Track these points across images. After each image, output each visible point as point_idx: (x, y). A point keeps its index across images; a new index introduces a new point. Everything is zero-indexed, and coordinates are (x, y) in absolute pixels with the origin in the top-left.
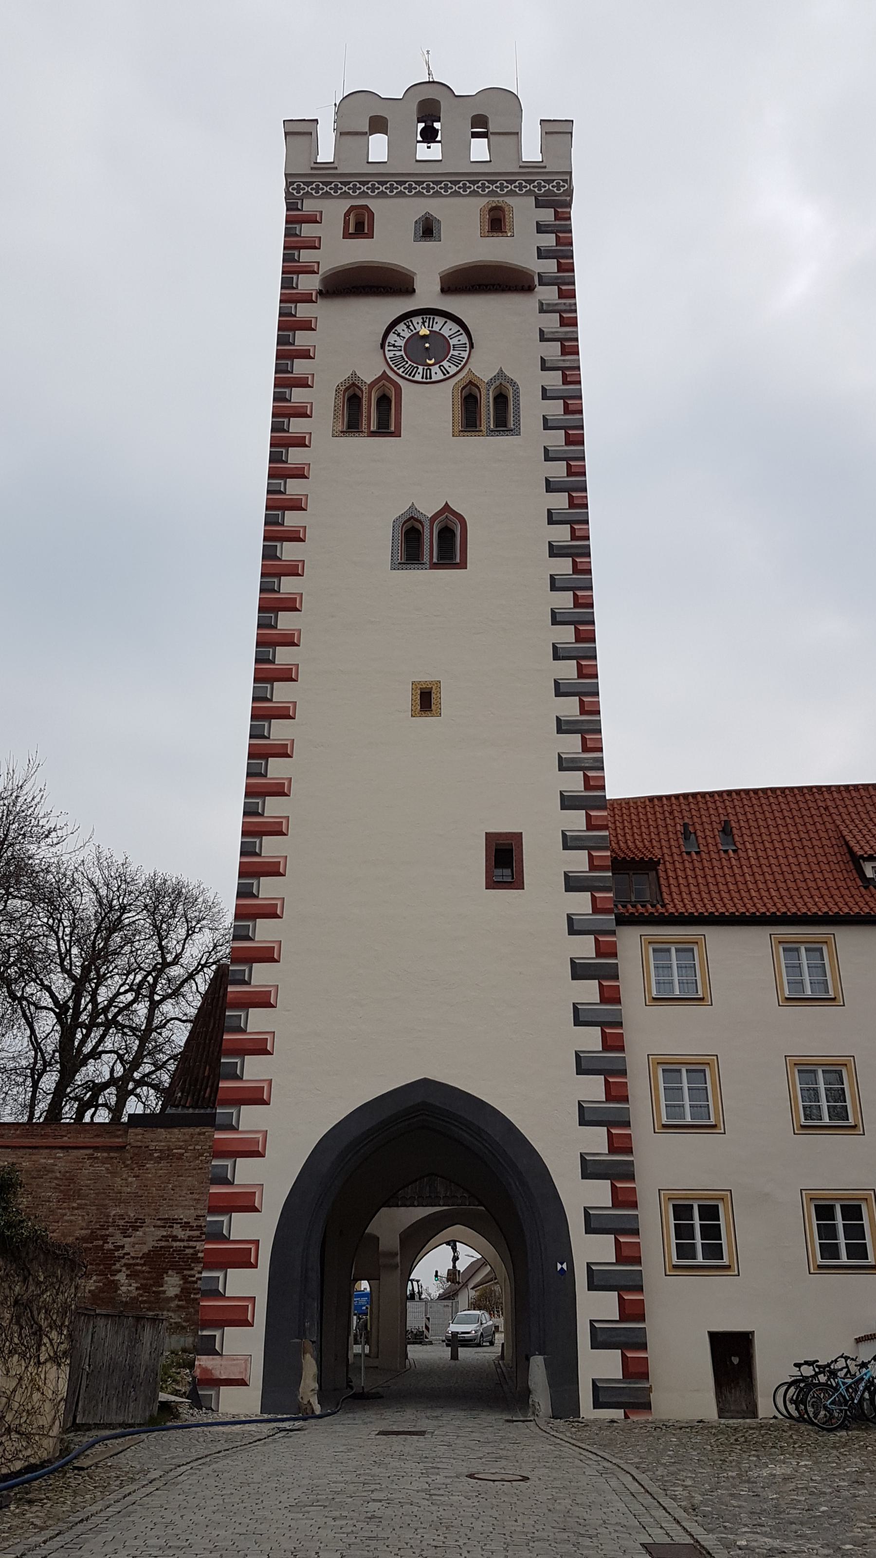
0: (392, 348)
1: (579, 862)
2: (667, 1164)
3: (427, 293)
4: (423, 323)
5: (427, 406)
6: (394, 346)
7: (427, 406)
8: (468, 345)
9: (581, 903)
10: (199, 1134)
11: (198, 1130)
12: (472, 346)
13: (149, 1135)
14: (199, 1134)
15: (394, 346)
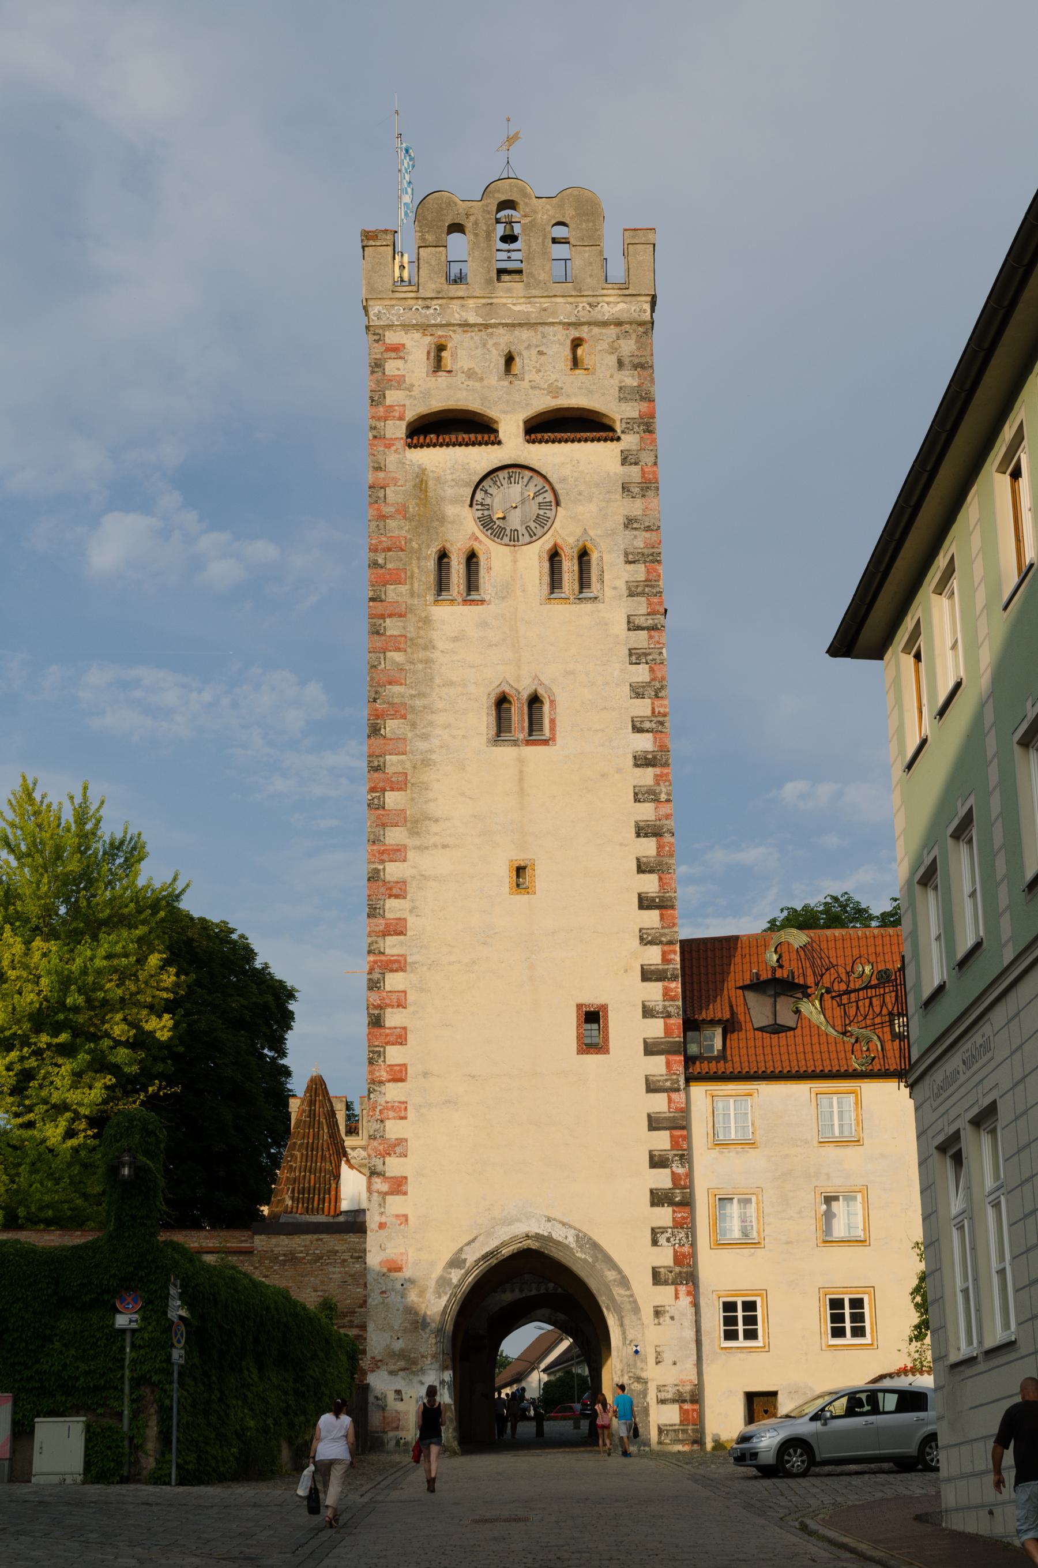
0: (479, 507)
1: (655, 1028)
2: (722, 1274)
3: (513, 446)
4: (509, 478)
5: (515, 568)
6: (482, 505)
7: (515, 568)
8: (553, 504)
9: (657, 1065)
10: (317, 1240)
11: (315, 1237)
12: (558, 504)
13: (274, 1240)
14: (317, 1240)
15: (482, 505)
